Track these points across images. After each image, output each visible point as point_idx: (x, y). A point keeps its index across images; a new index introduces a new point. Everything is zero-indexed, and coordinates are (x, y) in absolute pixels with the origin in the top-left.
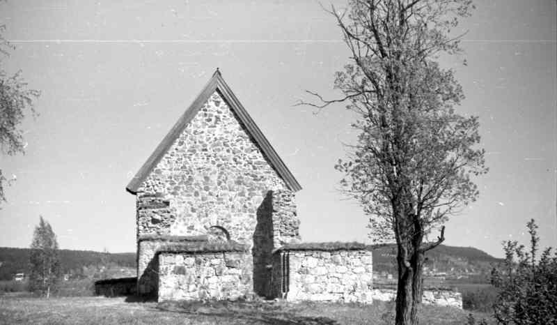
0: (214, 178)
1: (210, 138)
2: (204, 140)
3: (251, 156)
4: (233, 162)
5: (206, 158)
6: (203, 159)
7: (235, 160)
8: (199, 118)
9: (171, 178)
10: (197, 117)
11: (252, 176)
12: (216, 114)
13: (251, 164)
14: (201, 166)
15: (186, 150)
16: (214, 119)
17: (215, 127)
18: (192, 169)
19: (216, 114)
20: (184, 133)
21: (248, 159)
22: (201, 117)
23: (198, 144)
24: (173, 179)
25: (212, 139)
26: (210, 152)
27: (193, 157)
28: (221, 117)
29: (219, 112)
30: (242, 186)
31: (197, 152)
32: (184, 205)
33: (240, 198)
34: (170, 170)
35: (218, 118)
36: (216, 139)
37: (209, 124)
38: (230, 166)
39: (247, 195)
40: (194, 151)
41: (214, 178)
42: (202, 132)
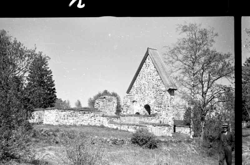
0: (147, 87)
2: (145, 73)
4: (152, 80)
7: (152, 79)
8: (144, 65)
10: (144, 66)
12: (148, 63)
16: (148, 65)
19: (148, 63)
23: (144, 75)
25: (147, 73)
26: (146, 77)
28: (150, 64)
29: (149, 63)
33: (153, 93)
34: (137, 85)
35: (149, 65)
36: (148, 73)
37: (147, 67)
39: (155, 92)
40: (142, 78)
41: (147, 87)
42: (145, 71)
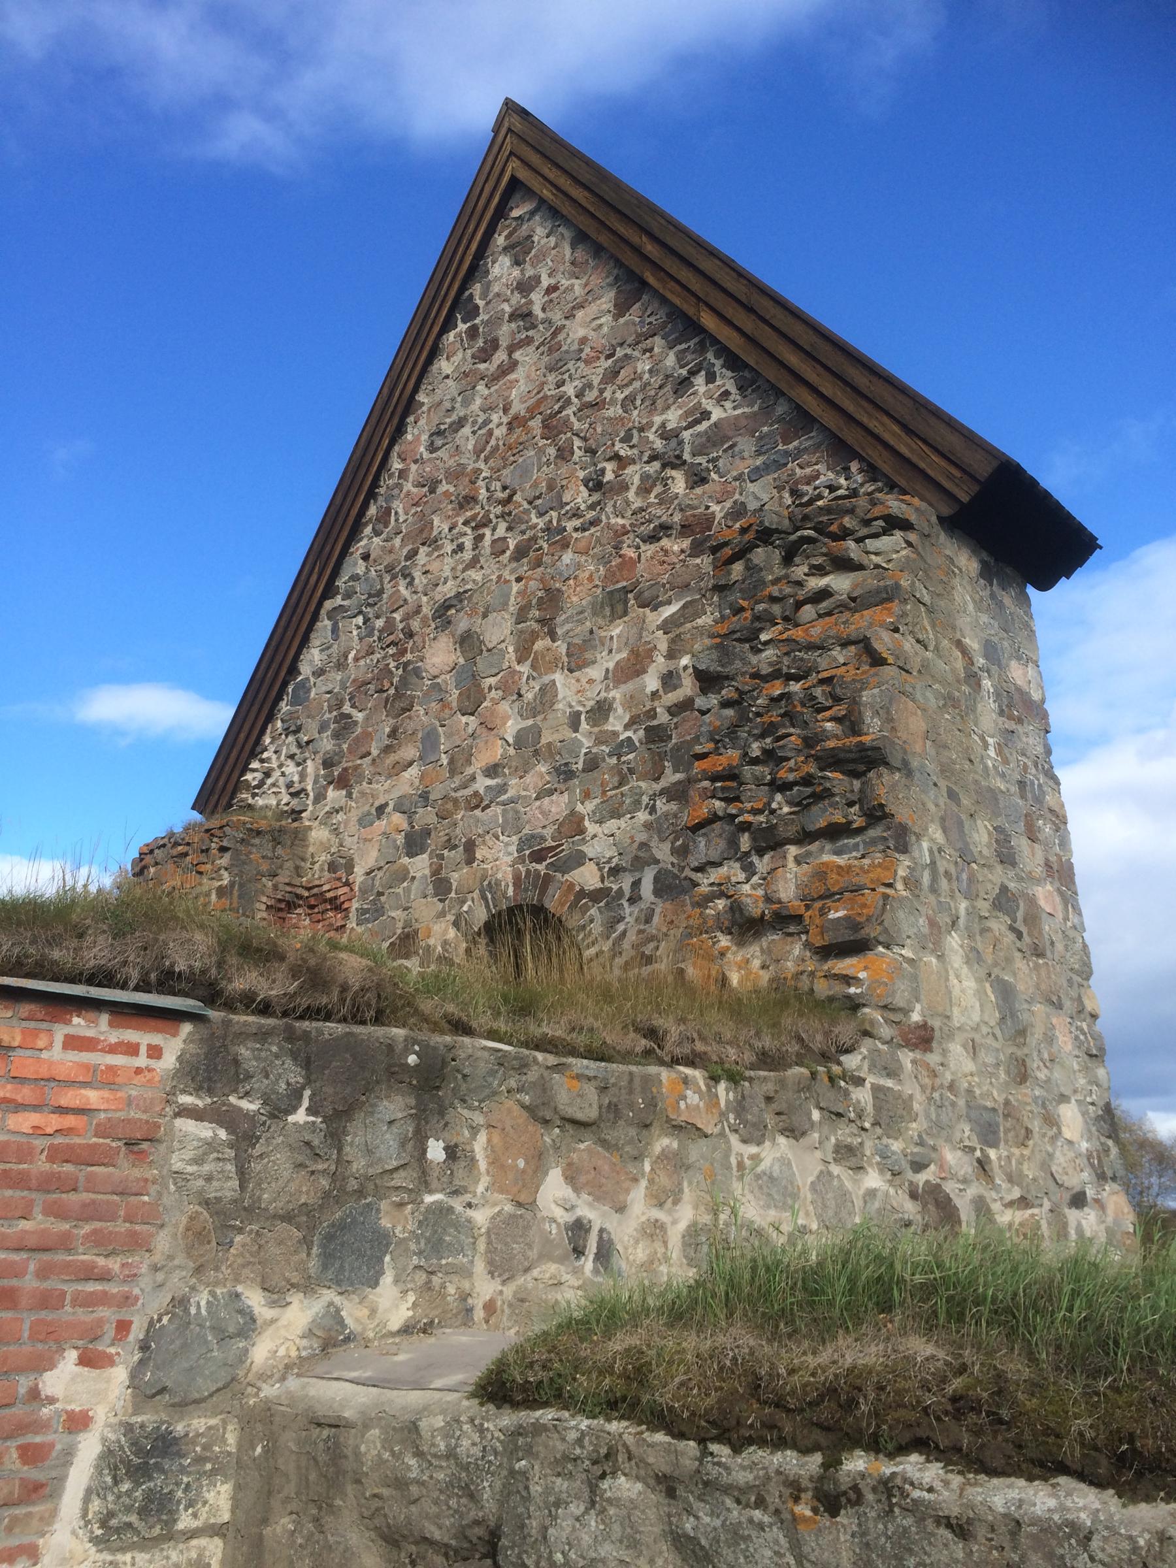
1: (490, 433)
3: (673, 417)
5: (468, 542)
6: (461, 548)
9: (340, 706)
10: (444, 366)
11: (686, 529)
13: (676, 462)
14: (448, 589)
15: (397, 541)
17: (513, 365)
18: (415, 624)
20: (396, 465)
21: (659, 444)
22: (460, 355)
24: (347, 708)
27: (422, 557)
30: (635, 611)
31: (440, 524)
32: (381, 825)
38: (570, 525)
